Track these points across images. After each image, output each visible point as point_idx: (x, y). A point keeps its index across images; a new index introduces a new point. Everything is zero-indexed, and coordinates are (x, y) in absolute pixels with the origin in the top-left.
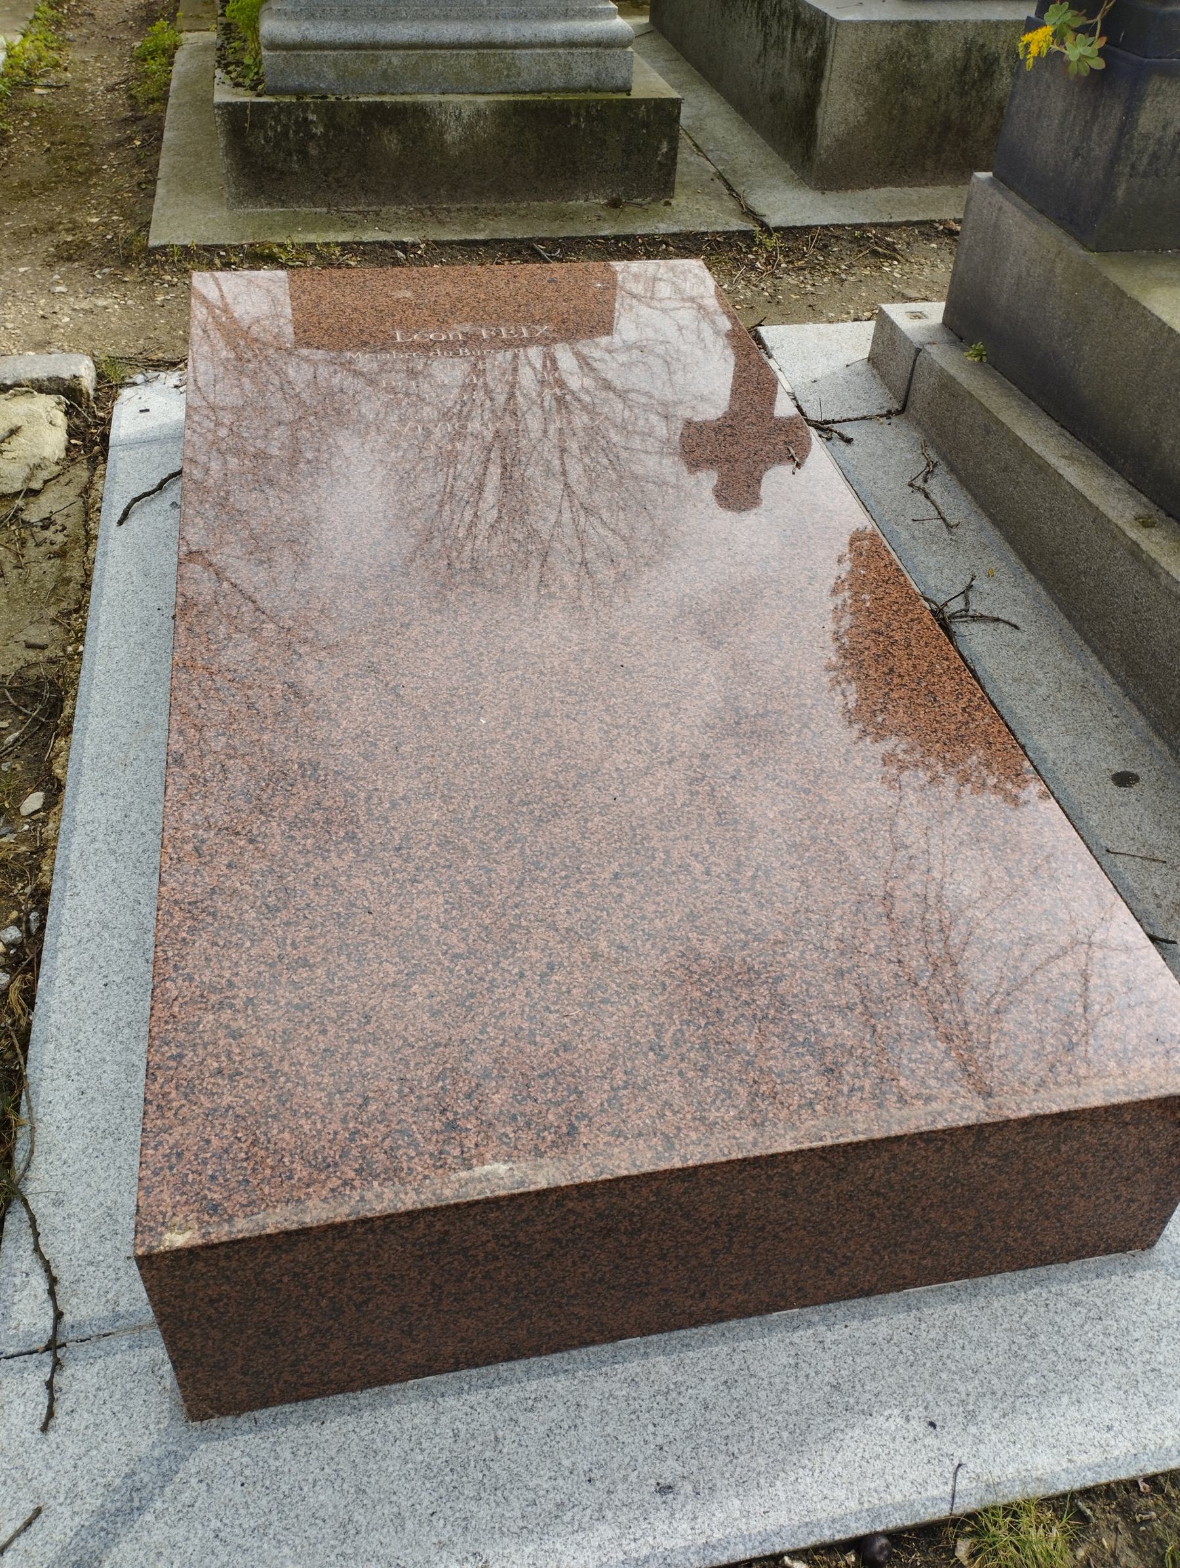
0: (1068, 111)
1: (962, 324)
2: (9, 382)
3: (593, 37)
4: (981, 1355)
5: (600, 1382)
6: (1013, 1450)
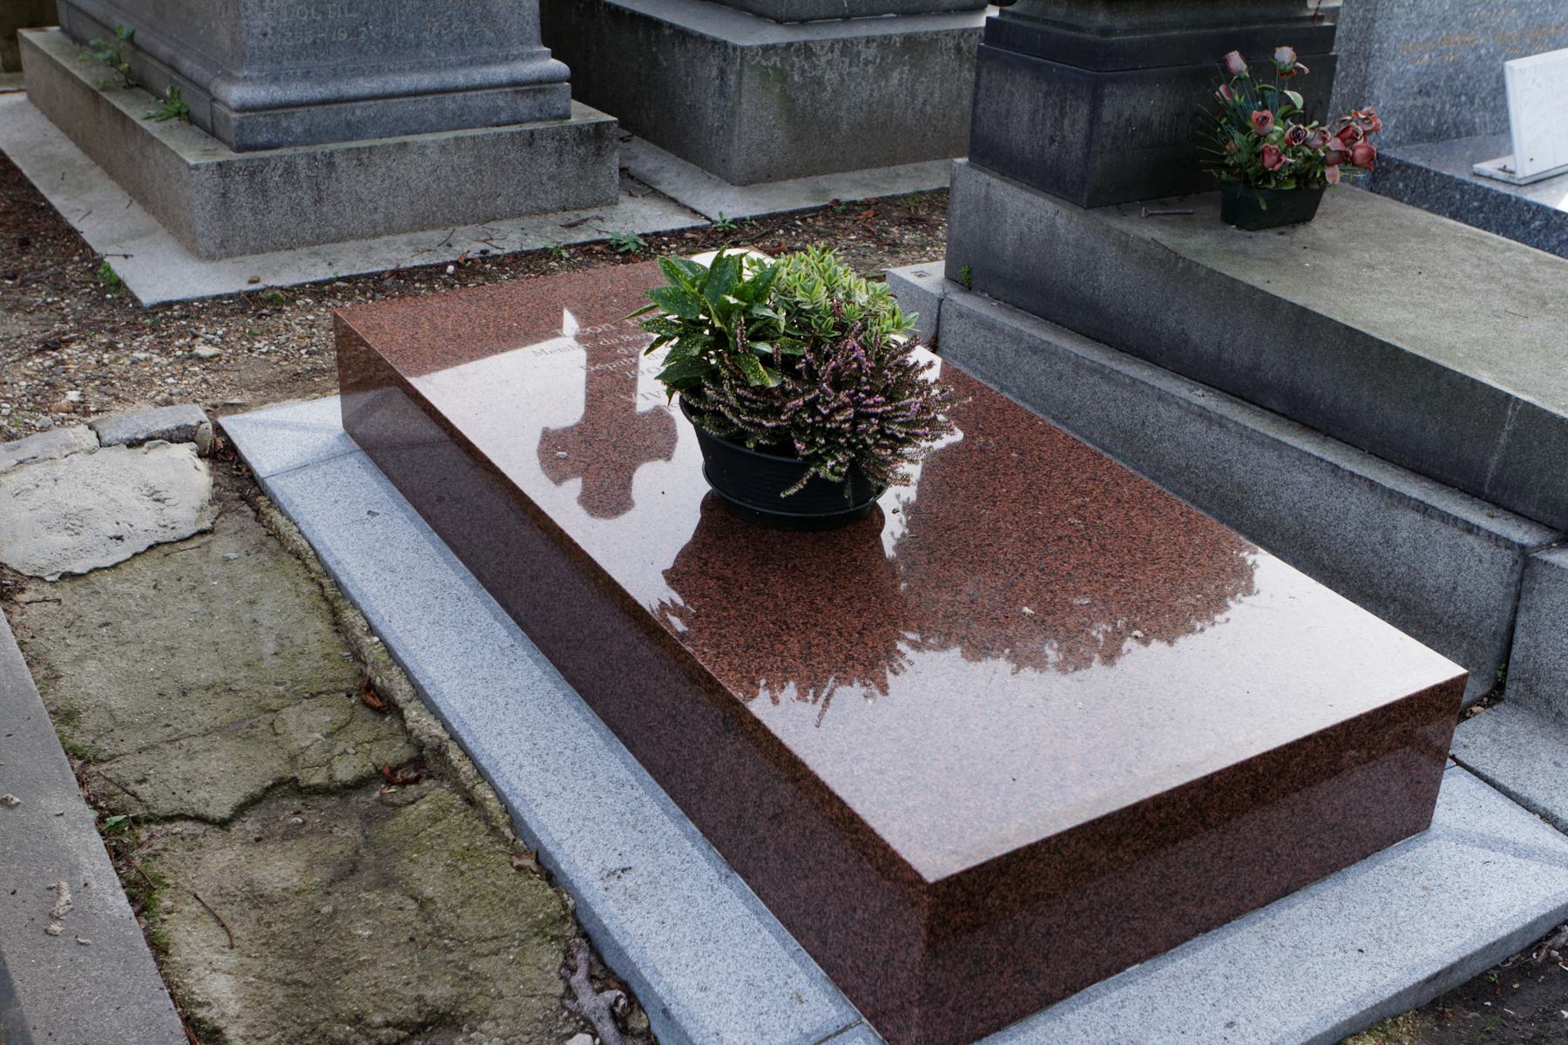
0: (1036, 111)
1: (964, 276)
2: (141, 437)
3: (535, 76)
4: (1366, 908)
5: (1155, 982)
6: (1413, 950)
